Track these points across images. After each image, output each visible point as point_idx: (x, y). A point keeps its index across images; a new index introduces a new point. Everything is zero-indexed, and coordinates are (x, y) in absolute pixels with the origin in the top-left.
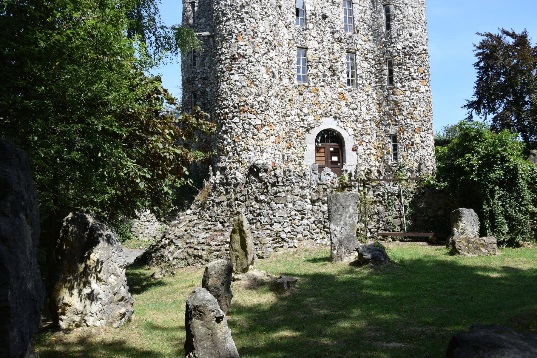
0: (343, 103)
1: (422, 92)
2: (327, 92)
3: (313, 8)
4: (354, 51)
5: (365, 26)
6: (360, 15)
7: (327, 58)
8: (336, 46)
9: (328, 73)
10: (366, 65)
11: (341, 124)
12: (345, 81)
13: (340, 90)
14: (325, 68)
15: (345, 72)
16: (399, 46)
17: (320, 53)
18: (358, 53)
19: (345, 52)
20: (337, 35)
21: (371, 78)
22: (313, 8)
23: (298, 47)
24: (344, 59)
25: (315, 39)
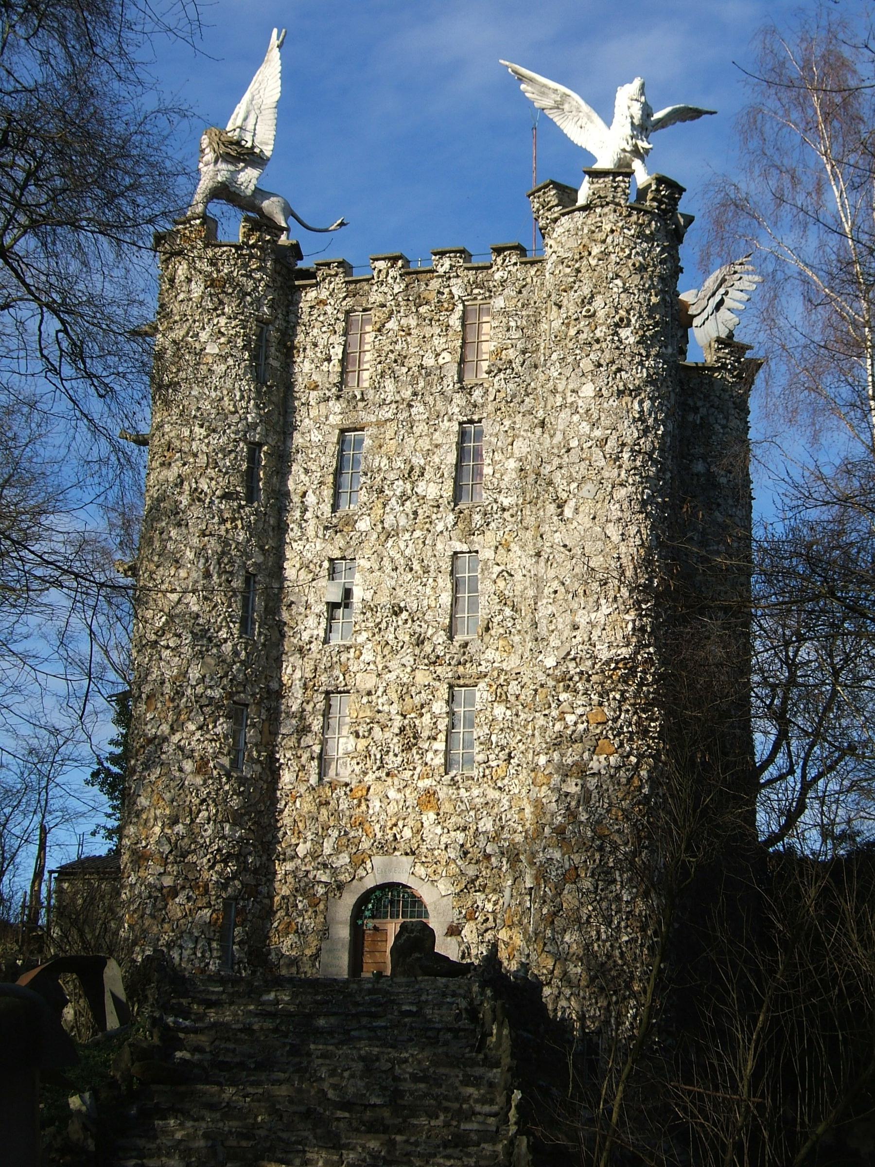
0: (429, 817)
1: (594, 774)
2: (392, 794)
3: (368, 596)
4: (471, 681)
5: (508, 612)
6: (492, 588)
7: (394, 709)
8: (422, 677)
9: (396, 745)
10: (499, 710)
11: (421, 870)
12: (439, 760)
13: (422, 784)
14: (388, 734)
15: (442, 737)
16: (550, 662)
17: (380, 701)
18: (482, 685)
19: (443, 691)
20: (428, 648)
21: (513, 744)
22: (368, 596)
23: (327, 693)
24: (439, 707)
25: (372, 666)
